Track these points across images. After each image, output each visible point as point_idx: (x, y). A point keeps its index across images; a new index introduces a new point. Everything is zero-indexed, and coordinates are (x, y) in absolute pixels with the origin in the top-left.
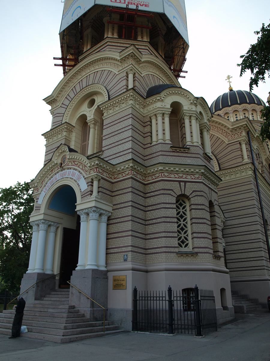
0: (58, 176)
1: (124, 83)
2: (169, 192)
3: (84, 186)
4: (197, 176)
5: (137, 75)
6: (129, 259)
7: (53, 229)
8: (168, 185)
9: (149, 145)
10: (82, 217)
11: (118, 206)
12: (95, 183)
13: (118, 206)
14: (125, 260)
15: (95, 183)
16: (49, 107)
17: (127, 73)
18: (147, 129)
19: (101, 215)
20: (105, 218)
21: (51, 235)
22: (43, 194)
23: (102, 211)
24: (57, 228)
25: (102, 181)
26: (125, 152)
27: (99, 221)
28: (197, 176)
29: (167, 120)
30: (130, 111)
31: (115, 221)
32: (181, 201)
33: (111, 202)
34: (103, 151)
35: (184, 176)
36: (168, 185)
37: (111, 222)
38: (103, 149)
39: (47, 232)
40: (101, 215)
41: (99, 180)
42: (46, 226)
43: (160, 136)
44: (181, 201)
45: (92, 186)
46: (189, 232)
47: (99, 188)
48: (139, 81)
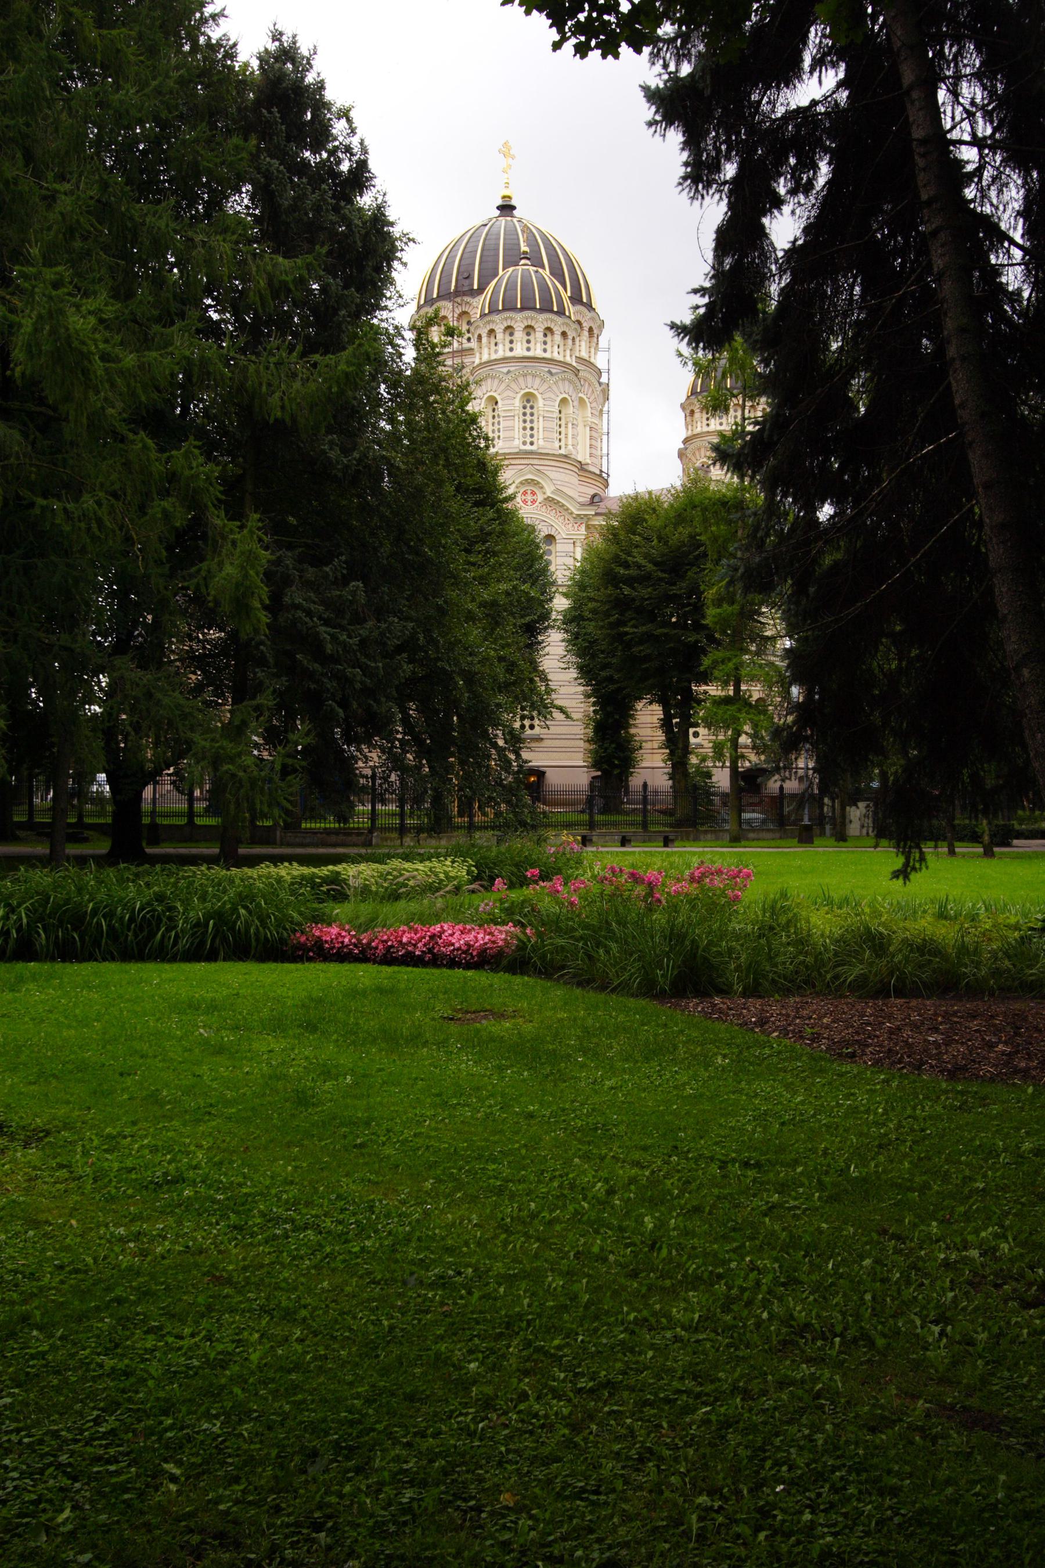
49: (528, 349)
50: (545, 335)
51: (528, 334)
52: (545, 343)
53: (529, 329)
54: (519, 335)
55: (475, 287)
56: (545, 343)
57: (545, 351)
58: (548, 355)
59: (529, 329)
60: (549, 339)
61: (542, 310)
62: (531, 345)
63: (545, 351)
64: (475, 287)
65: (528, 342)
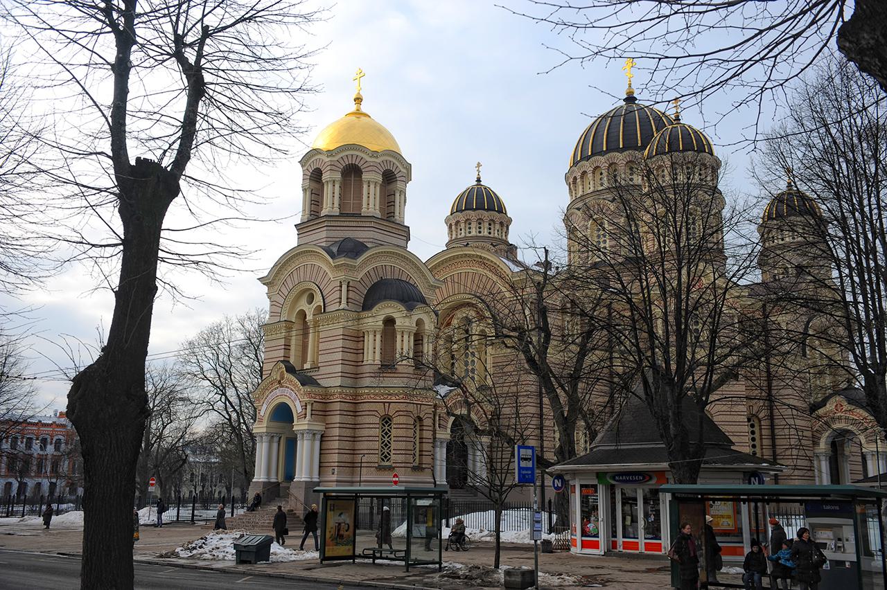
0: (278, 392)
1: (337, 295)
2: (374, 413)
3: (299, 410)
4: (401, 396)
5: (351, 284)
6: (336, 473)
7: (276, 439)
8: (373, 406)
9: (360, 363)
10: (298, 436)
11: (330, 426)
12: (309, 407)
13: (330, 426)
14: (333, 474)
15: (309, 407)
16: (266, 288)
17: (341, 282)
18: (360, 345)
19: (314, 434)
20: (318, 437)
21: (275, 445)
22: (265, 406)
23: (315, 432)
24: (280, 438)
25: (315, 404)
26: (336, 375)
27: (313, 440)
28: (401, 396)
29: (378, 337)
30: (341, 332)
31: (326, 439)
32: (387, 419)
33: (324, 421)
34: (319, 368)
35: (389, 397)
36: (373, 406)
37: (325, 439)
38: (319, 365)
39: (270, 442)
40: (314, 434)
41: (312, 404)
42: (269, 437)
43: (370, 358)
44: (387, 419)
45: (306, 409)
46: (392, 448)
47: (312, 410)
48: (355, 290)
49: (480, 232)
50: (490, 224)
51: (480, 224)
52: (490, 229)
53: (480, 221)
54: (474, 225)
55: (621, 146)
56: (490, 229)
57: (490, 233)
58: (492, 235)
59: (480, 221)
60: (492, 227)
61: (488, 210)
62: (482, 230)
63: (490, 233)
64: (621, 146)
65: (480, 228)
